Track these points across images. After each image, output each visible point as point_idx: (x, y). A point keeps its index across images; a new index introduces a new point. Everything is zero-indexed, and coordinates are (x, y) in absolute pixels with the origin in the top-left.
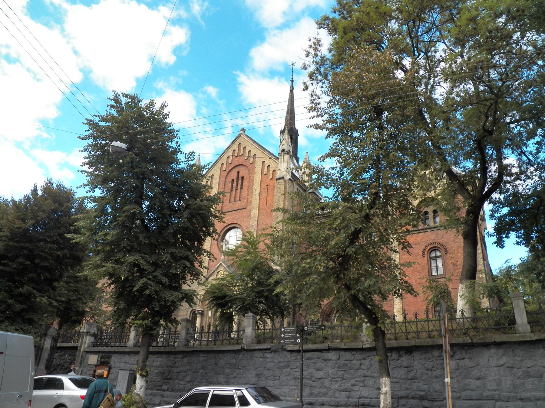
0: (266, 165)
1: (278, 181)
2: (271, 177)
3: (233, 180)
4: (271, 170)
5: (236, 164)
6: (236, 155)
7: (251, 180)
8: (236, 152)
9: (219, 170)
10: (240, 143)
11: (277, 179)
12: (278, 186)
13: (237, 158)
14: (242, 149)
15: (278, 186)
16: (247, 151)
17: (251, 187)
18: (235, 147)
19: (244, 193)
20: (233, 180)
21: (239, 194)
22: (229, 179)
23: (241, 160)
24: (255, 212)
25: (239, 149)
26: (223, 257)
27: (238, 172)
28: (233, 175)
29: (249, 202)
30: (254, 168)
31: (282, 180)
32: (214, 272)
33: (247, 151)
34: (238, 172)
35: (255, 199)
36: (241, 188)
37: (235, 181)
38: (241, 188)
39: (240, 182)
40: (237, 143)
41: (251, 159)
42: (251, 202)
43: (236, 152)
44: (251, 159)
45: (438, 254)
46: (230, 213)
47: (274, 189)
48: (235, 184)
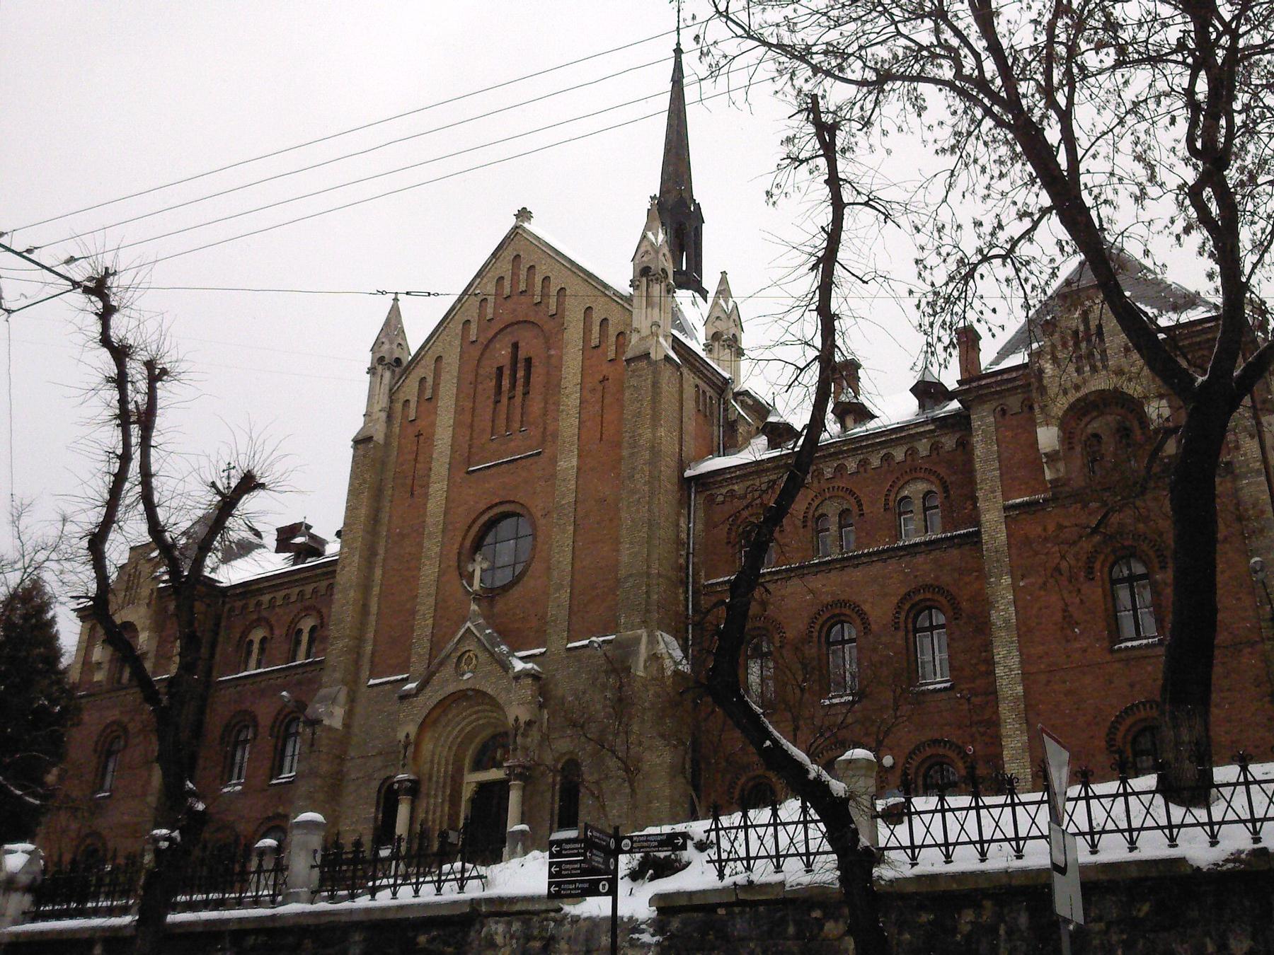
0: (596, 318)
2: (611, 355)
3: (500, 369)
4: (612, 331)
5: (509, 318)
6: (507, 291)
7: (554, 368)
8: (507, 283)
9: (457, 342)
10: (518, 256)
11: (628, 361)
12: (634, 382)
13: (509, 301)
15: (634, 382)
16: (538, 280)
17: (553, 386)
18: (505, 268)
19: (536, 406)
20: (500, 369)
21: (518, 411)
22: (488, 369)
24: (568, 463)
25: (515, 274)
26: (474, 607)
27: (515, 346)
28: (502, 353)
29: (548, 436)
30: (562, 328)
31: (644, 364)
32: (448, 656)
33: (538, 280)
34: (515, 346)
35: (569, 425)
36: (526, 393)
37: (507, 372)
38: (526, 393)
39: (521, 374)
40: (508, 254)
41: (553, 301)
42: (555, 435)
43: (507, 283)
44: (553, 301)
45: (1139, 569)
47: (621, 391)
48: (506, 383)
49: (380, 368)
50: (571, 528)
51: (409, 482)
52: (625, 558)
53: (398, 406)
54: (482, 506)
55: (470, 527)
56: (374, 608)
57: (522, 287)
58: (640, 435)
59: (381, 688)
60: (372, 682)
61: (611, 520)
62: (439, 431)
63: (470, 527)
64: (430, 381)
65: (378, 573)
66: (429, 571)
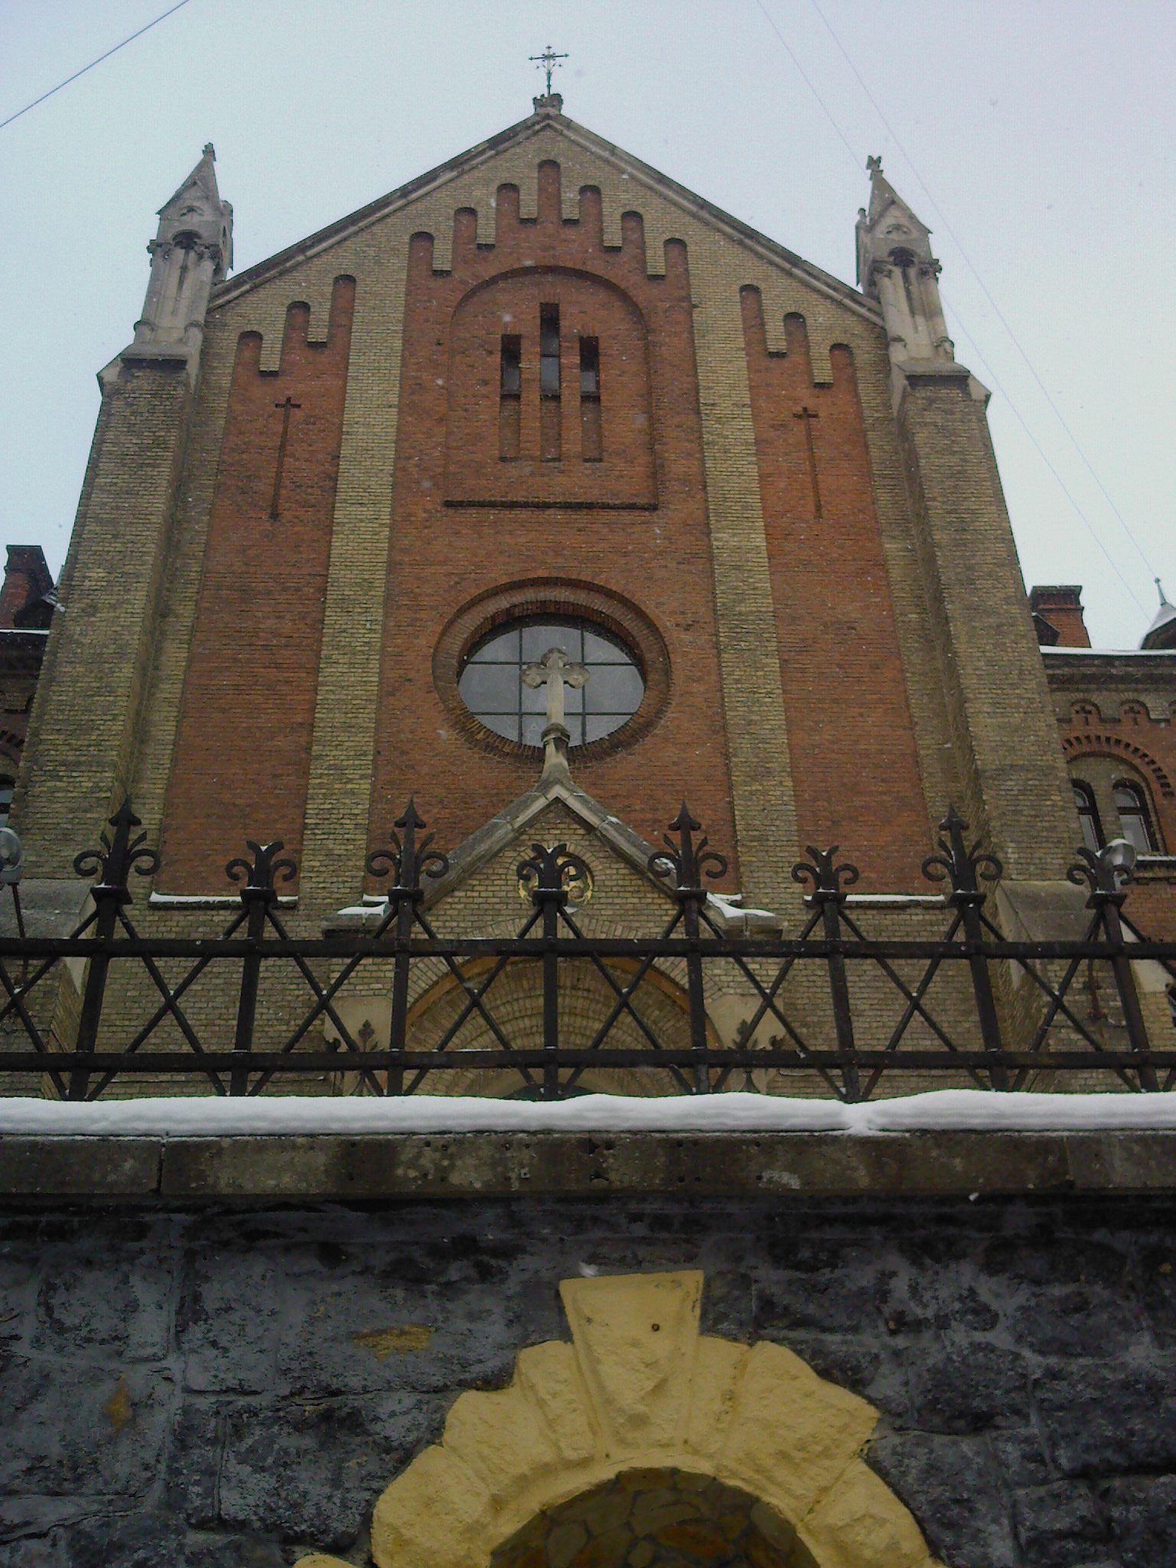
1: (922, 393)
14: (570, 195)
19: (626, 424)
23: (574, 249)
24: (742, 540)
28: (515, 313)
32: (494, 856)
40: (530, 153)
46: (524, 514)
49: (179, 253)
50: (774, 663)
51: (264, 486)
52: (984, 725)
53: (228, 340)
54: (499, 575)
55: (463, 610)
56: (164, 728)
57: (569, 212)
58: (973, 512)
59: (202, 916)
60: (155, 897)
61: (875, 667)
62: (355, 412)
63: (463, 610)
64: (321, 312)
65: (175, 656)
66: (349, 677)
